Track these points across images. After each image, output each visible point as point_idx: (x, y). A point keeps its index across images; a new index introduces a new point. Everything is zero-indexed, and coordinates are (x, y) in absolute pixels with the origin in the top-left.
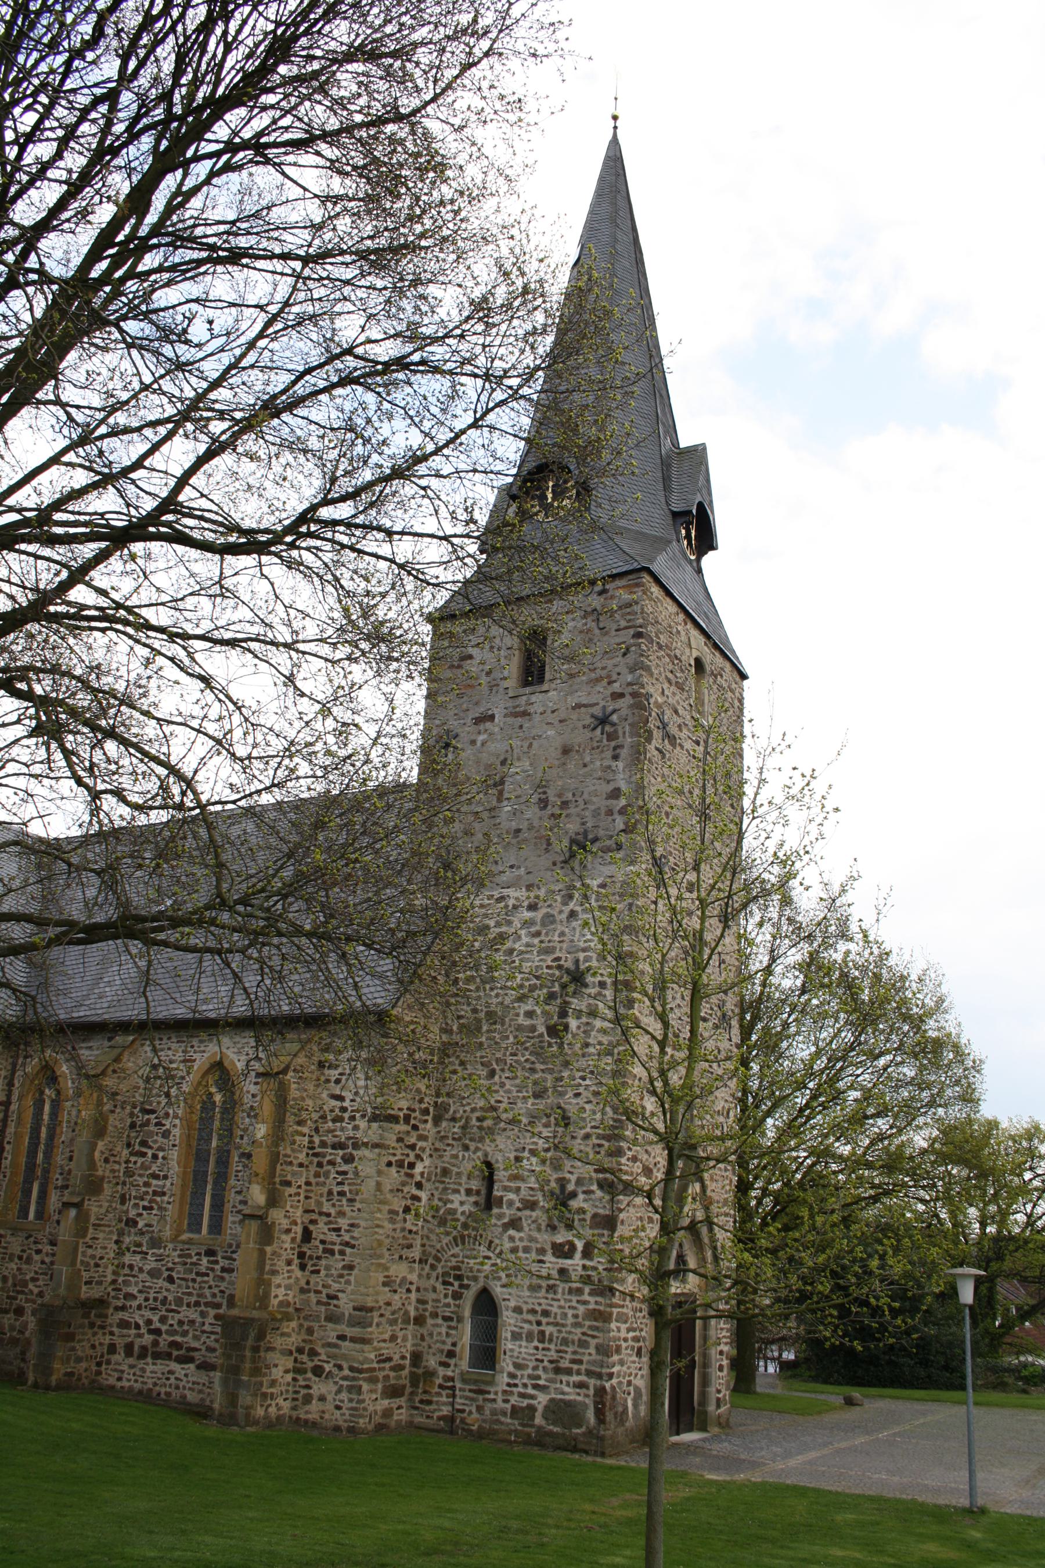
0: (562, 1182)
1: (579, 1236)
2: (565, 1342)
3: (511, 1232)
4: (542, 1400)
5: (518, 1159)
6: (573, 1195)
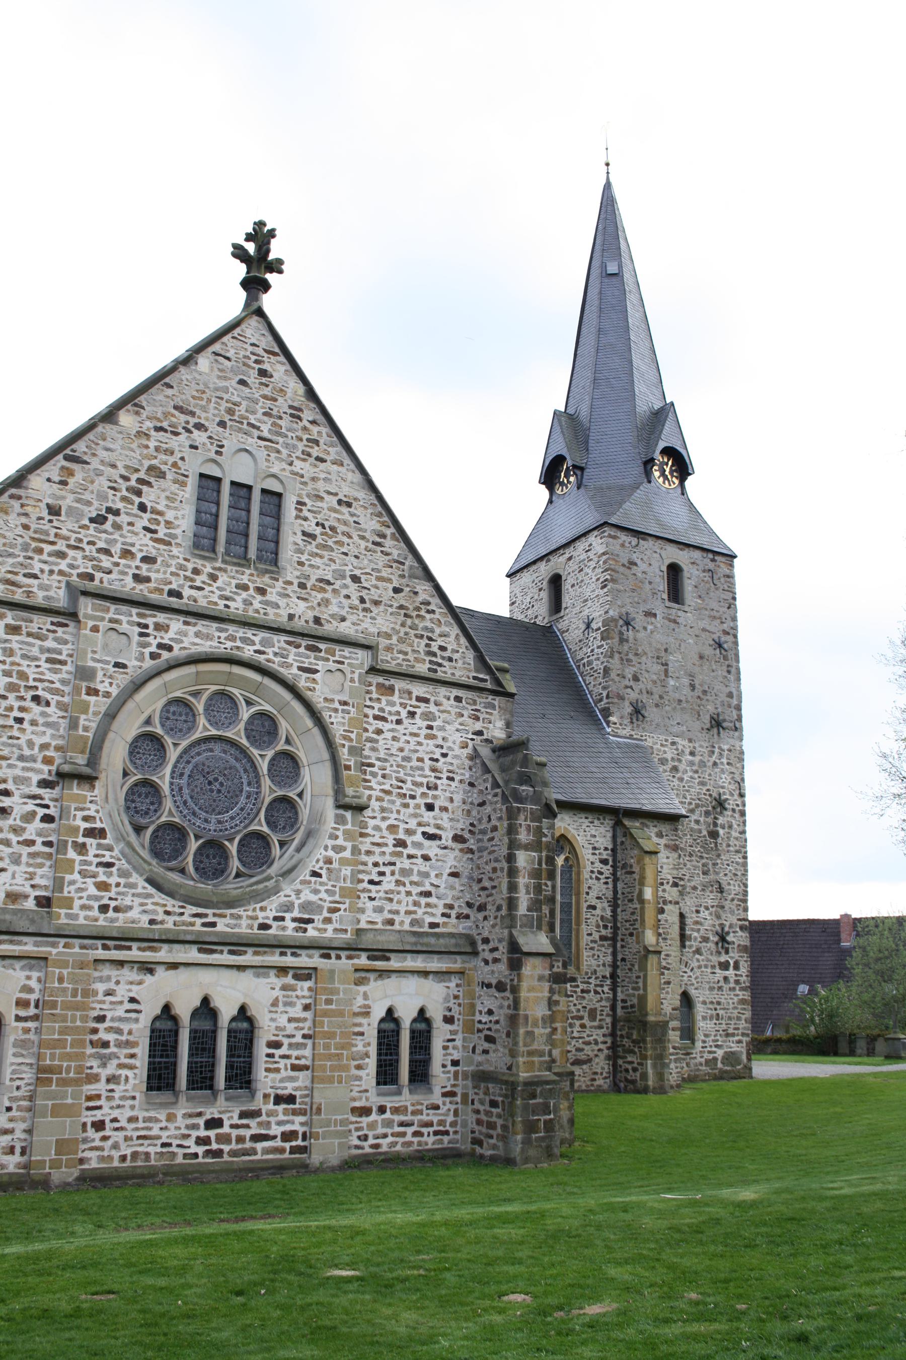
0: (722, 926)
1: (732, 958)
2: (730, 1018)
3: (697, 956)
4: (720, 1053)
5: (698, 912)
6: (728, 933)
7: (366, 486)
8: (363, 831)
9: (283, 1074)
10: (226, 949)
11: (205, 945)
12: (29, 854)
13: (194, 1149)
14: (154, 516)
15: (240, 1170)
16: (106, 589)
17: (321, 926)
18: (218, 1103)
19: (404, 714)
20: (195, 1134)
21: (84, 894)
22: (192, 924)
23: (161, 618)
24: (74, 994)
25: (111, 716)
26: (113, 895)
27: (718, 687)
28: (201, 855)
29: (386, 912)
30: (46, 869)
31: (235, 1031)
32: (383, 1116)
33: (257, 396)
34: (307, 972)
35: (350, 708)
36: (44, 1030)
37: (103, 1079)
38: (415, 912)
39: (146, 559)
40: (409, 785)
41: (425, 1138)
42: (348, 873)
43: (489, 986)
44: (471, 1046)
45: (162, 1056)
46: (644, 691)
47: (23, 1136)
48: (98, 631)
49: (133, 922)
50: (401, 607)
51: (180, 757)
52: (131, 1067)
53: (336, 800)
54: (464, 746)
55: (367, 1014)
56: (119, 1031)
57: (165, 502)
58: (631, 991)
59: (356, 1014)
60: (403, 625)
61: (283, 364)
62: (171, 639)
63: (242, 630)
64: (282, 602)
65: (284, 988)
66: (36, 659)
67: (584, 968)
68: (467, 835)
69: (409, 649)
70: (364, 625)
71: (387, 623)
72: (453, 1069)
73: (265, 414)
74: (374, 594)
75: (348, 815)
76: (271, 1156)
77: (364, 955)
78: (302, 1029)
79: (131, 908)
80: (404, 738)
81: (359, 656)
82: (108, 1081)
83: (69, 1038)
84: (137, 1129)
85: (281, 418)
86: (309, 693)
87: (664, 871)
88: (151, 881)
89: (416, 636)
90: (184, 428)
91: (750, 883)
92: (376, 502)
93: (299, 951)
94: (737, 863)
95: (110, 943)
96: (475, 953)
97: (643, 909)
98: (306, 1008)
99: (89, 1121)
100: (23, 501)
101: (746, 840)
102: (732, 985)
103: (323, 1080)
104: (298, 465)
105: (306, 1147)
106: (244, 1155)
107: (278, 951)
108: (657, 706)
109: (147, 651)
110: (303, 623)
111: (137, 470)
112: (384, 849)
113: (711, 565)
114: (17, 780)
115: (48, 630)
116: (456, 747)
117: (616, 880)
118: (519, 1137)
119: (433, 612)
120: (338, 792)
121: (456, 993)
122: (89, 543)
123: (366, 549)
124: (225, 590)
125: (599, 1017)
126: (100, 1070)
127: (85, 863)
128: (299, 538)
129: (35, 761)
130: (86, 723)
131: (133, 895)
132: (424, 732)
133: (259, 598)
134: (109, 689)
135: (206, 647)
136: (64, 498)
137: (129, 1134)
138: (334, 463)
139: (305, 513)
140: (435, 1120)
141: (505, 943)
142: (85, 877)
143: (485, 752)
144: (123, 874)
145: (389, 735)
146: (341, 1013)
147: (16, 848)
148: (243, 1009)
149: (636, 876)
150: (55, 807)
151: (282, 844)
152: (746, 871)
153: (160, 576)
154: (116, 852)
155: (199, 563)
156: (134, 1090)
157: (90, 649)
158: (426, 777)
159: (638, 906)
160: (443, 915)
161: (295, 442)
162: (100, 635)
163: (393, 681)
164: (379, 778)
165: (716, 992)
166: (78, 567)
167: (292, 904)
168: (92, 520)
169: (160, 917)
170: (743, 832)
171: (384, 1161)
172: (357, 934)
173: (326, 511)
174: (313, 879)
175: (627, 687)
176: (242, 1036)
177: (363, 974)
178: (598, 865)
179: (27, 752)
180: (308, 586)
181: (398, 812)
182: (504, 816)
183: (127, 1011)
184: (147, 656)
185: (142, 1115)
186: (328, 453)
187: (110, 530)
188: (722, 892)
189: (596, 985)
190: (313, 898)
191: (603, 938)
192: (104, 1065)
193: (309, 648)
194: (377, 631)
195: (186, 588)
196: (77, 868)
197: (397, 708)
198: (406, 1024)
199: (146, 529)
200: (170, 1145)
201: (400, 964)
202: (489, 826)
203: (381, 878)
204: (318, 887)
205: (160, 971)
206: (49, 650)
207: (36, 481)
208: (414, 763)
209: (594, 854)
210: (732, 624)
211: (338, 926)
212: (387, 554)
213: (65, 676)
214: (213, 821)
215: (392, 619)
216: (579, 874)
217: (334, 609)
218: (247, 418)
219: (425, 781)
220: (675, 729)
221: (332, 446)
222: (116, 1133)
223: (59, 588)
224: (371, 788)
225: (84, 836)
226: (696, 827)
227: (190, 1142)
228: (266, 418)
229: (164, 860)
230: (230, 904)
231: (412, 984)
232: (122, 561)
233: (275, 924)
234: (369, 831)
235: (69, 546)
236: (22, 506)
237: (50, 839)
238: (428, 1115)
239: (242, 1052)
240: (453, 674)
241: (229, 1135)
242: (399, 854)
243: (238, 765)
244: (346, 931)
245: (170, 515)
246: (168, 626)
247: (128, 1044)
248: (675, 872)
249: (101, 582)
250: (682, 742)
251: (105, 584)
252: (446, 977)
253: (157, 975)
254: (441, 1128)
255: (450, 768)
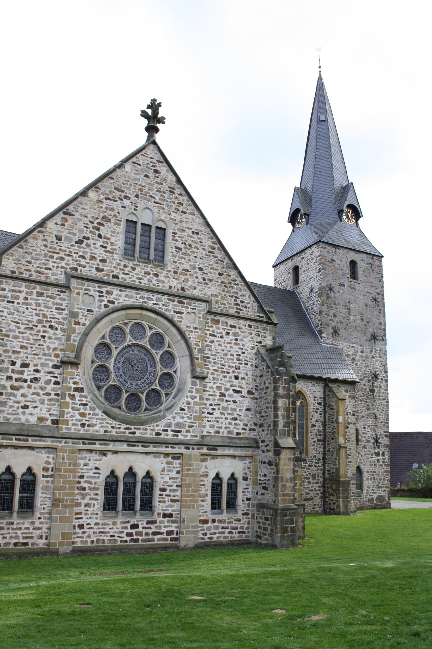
0: (376, 435)
1: (381, 450)
2: (380, 479)
3: (364, 449)
4: (375, 496)
5: (364, 428)
6: (379, 438)
7: (206, 225)
8: (205, 389)
9: (167, 503)
10: (140, 444)
11: (130, 443)
12: (48, 399)
13: (125, 538)
14: (105, 240)
15: (147, 548)
16: (83, 275)
17: (185, 434)
18: (137, 517)
19: (224, 333)
20: (126, 531)
21: (74, 418)
22: (124, 433)
23: (109, 288)
24: (70, 465)
25: (86, 334)
26: (87, 419)
27: (374, 320)
28: (128, 400)
29: (216, 427)
30: (56, 406)
31: (145, 483)
32: (214, 524)
33: (153, 182)
34: (178, 455)
35: (198, 330)
36: (56, 482)
37: (83, 505)
38: (229, 428)
39: (102, 261)
40: (227, 367)
41: (234, 535)
42: (198, 409)
43: (264, 463)
44: (256, 491)
45: (110, 495)
46: (339, 322)
47: (46, 531)
48: (79, 295)
49: (96, 432)
50: (223, 282)
51: (119, 354)
52: (96, 500)
53: (192, 374)
54: (253, 348)
55: (207, 476)
56: (90, 483)
57: (110, 233)
58: (332, 466)
59: (201, 476)
60: (223, 291)
61: (166, 167)
62: (114, 298)
63: (147, 294)
64: (166, 280)
65: (167, 463)
66: (51, 308)
67: (310, 455)
68: (254, 391)
69: (226, 302)
70: (205, 291)
71: (216, 290)
72: (247, 502)
73: (157, 191)
74: (210, 276)
75: (198, 381)
76: (161, 542)
77: (205, 448)
78: (176, 482)
79: (96, 425)
80: (224, 345)
81: (203, 306)
82: (85, 506)
83: (67, 486)
84: (99, 528)
85: (165, 193)
86: (179, 323)
87: (348, 408)
88: (105, 412)
89: (230, 296)
90: (119, 198)
91: (390, 414)
92: (210, 232)
93: (174, 446)
94: (384, 405)
95: (86, 441)
96: (258, 447)
97: (338, 427)
98: (178, 472)
99: (77, 524)
100: (45, 234)
101: (388, 394)
102: (381, 463)
103: (186, 507)
104: (173, 215)
105: (178, 538)
106: (148, 541)
107: (165, 445)
108: (345, 329)
109: (102, 304)
110: (176, 290)
111: (97, 219)
112: (215, 397)
113: (371, 261)
114: (42, 365)
115: (56, 294)
116: (249, 349)
117: (325, 413)
118: (279, 535)
119: (238, 284)
120: (193, 370)
121: (249, 466)
122: (75, 253)
123: (206, 255)
124: (139, 275)
125: (317, 478)
126: (81, 501)
127: (74, 404)
128: (174, 250)
129: (51, 356)
130: (74, 338)
131: (97, 419)
132: (234, 342)
133: (155, 278)
134: (85, 322)
135: (130, 302)
136: (63, 232)
137: (95, 530)
138: (190, 214)
139: (177, 238)
140: (239, 526)
141: (272, 443)
142: (74, 410)
143: (263, 351)
144: (92, 409)
145: (217, 343)
146: (194, 475)
147: (42, 397)
148: (148, 473)
149: (335, 411)
150: (60, 377)
151: (166, 395)
152: (388, 408)
153: (109, 268)
154: (89, 399)
155: (127, 262)
156: (97, 510)
157: (76, 303)
158: (234, 363)
159: (336, 425)
160: (243, 429)
161: (171, 204)
162: (80, 296)
163: (218, 318)
164: (212, 364)
165: (373, 466)
166: (70, 265)
167: (171, 423)
168: (76, 242)
169: (109, 429)
170: (387, 390)
171: (214, 545)
172: (202, 438)
173: (186, 237)
174: (181, 412)
175: (330, 320)
176: (148, 485)
177: (205, 457)
178: (317, 405)
179: (47, 352)
180: (178, 273)
181: (221, 380)
182: (272, 382)
183: (94, 473)
184: (103, 306)
185: (101, 522)
186: (187, 209)
187: (85, 247)
188: (376, 419)
189: (315, 463)
190: (181, 421)
191: (319, 440)
192: (83, 498)
193: (178, 302)
194: (211, 294)
195: (121, 274)
196: (71, 406)
197: (221, 330)
198: (225, 480)
199: (102, 246)
200: (114, 536)
201: (222, 452)
202: (265, 387)
203: (213, 411)
204: (184, 415)
205: (109, 455)
206: (57, 304)
207: (50, 224)
208: (229, 357)
209: (314, 400)
210: (381, 290)
211: (193, 434)
212: (216, 257)
213: (64, 316)
214: (134, 384)
215: (218, 288)
216: (307, 409)
217: (190, 283)
218: (149, 193)
219: (234, 365)
220: (354, 340)
221: (189, 205)
222: (89, 530)
223: (61, 274)
224: (208, 369)
225: (74, 391)
226: (364, 387)
227: (124, 535)
228: (157, 193)
229: (111, 402)
230: (142, 423)
231: (228, 461)
232: (91, 262)
233: (163, 433)
234: (208, 389)
235: (66, 255)
236: (44, 236)
237: (58, 392)
238: (235, 524)
239: (148, 493)
240: (247, 314)
241: (142, 532)
242: (222, 400)
243: (145, 358)
244: (197, 436)
245: (113, 240)
246: (112, 292)
247: (94, 489)
248: (354, 409)
249: (81, 271)
250: (357, 347)
251: (83, 273)
252: (244, 458)
253: (108, 456)
254: (242, 530)
255: (246, 359)
